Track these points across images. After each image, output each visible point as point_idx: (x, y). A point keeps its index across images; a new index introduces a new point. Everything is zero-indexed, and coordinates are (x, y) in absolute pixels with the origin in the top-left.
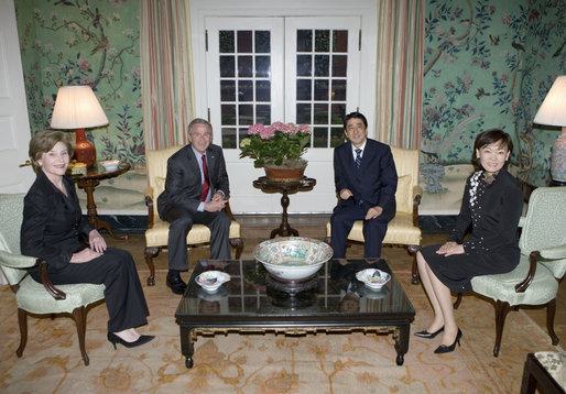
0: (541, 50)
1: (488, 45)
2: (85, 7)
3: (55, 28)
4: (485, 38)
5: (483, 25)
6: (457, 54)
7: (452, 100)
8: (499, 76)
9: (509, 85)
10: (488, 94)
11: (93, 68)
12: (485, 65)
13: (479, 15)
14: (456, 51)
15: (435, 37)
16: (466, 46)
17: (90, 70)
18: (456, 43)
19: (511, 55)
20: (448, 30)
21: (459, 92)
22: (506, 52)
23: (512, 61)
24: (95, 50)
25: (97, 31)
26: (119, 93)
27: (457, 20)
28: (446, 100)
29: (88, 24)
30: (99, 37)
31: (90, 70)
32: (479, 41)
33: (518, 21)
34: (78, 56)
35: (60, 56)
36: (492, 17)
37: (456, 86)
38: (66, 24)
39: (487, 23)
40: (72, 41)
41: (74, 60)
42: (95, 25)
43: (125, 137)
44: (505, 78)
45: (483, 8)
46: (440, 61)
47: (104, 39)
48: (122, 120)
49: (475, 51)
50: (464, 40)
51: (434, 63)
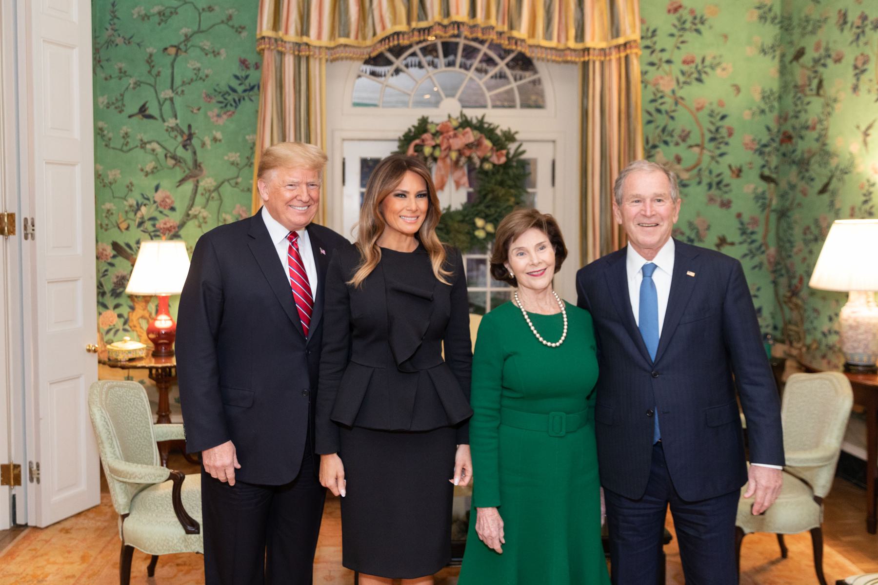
0: (801, 185)
1: (727, 177)
2: (172, 122)
3: (125, 148)
4: (722, 167)
5: (718, 152)
8: (746, 218)
9: (760, 230)
10: (732, 244)
11: (176, 205)
12: (726, 204)
13: (713, 139)
16: (697, 180)
17: (173, 209)
19: (760, 190)
20: (672, 158)
22: (752, 186)
23: (760, 198)
24: (182, 181)
25: (187, 155)
27: (683, 146)
29: (175, 145)
30: (190, 163)
31: (173, 209)
32: (715, 172)
33: (765, 146)
34: (157, 188)
35: (130, 187)
36: (731, 140)
38: (143, 144)
39: (724, 148)
40: (149, 167)
41: (150, 193)
42: (184, 146)
44: (755, 221)
45: (717, 130)
47: (197, 165)
49: (710, 186)
50: (695, 171)
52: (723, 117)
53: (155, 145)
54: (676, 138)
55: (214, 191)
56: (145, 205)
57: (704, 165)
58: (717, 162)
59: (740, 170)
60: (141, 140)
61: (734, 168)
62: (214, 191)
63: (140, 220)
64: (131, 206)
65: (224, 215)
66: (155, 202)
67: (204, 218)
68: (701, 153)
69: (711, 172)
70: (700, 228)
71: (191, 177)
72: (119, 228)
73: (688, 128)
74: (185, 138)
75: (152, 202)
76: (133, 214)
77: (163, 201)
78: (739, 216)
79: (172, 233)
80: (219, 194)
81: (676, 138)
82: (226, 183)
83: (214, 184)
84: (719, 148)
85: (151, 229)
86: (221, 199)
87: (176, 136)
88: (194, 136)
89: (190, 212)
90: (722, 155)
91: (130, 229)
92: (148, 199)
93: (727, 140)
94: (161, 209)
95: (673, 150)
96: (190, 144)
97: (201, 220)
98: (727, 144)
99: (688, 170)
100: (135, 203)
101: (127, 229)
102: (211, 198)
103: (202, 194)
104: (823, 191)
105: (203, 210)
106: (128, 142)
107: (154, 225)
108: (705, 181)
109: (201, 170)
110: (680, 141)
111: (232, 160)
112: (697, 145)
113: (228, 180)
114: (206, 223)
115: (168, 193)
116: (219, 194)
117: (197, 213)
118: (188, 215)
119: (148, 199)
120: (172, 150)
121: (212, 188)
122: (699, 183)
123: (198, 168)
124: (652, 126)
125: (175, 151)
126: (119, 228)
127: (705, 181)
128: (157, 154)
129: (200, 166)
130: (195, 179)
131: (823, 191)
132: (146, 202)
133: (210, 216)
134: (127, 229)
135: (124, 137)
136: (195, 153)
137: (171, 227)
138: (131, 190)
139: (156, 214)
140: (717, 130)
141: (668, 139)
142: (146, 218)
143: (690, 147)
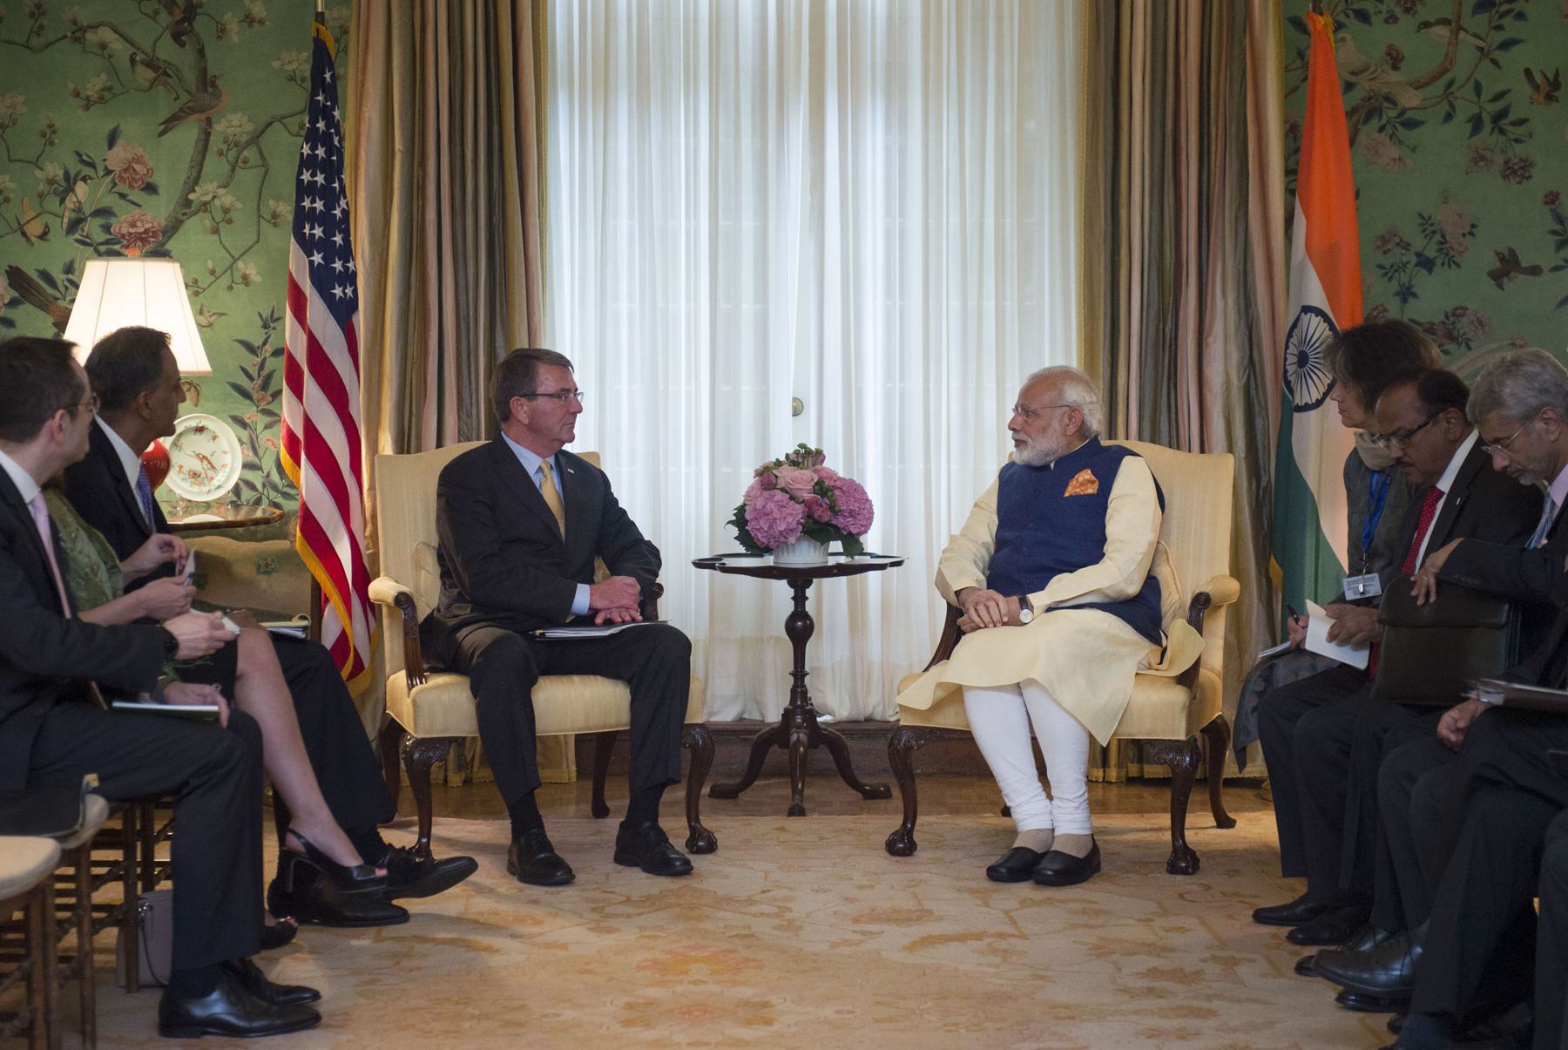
1: (1521, 100)
3: (35, 41)
5: (1499, 37)
6: (1411, 136)
7: (1406, 294)
10: (1535, 271)
11: (159, 179)
12: (1518, 171)
14: (1411, 124)
16: (1445, 107)
17: (151, 189)
18: (1410, 99)
21: (1426, 264)
24: (170, 123)
26: (249, 267)
27: (1406, 22)
30: (191, 78)
31: (151, 189)
34: (112, 140)
35: (49, 136)
37: (1418, 243)
38: (78, 33)
39: (1512, 28)
40: (93, 87)
41: (96, 151)
42: (176, 37)
43: (264, 420)
47: (207, 82)
48: (251, 362)
49: (1476, 124)
50: (1438, 88)
53: (106, 34)
55: (248, 144)
56: (84, 179)
57: (1460, 72)
58: (1495, 63)
59: (1555, 84)
60: (74, 22)
61: (1538, 78)
62: (248, 144)
63: (74, 215)
64: (51, 182)
65: (272, 203)
66: (108, 172)
67: (226, 211)
68: (1454, 41)
69: (1478, 89)
70: (1448, 230)
71: (193, 111)
72: (24, 234)
74: (178, 16)
75: (101, 173)
76: (57, 200)
77: (126, 170)
78: (1552, 198)
79: (149, 247)
80: (261, 153)
82: (277, 125)
83: (249, 127)
84: (1499, 28)
85: (99, 236)
86: (264, 164)
87: (156, 13)
88: (199, 11)
89: (192, 196)
90: (1506, 45)
91: (50, 236)
92: (92, 165)
94: (122, 188)
96: (191, 31)
97: (219, 216)
99: (1418, 86)
100: (61, 173)
101: (44, 236)
102: (240, 164)
103: (221, 153)
105: (221, 191)
106: (41, 27)
107: (107, 228)
108: (1464, 111)
109: (217, 94)
110: (1398, 11)
111: (289, 68)
112: (1444, 22)
113: (281, 119)
114: (230, 222)
115: (140, 151)
116: (261, 153)
117: (208, 198)
118: (187, 203)
119: (92, 165)
120: (147, 45)
121: (244, 138)
122: (1449, 117)
123: (210, 90)
125: (154, 50)
126: (24, 234)
127: (1464, 111)
128: (110, 56)
129: (213, 85)
130: (203, 116)
132: (87, 171)
133: (239, 205)
134: (44, 236)
135: (32, 15)
136: (201, 52)
137: (146, 231)
138: (52, 144)
139: (110, 201)
142: (87, 211)
143: (1426, 25)
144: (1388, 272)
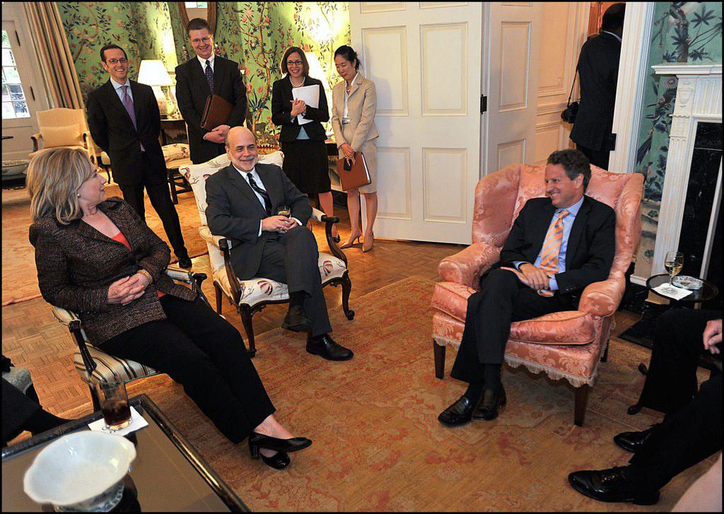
5: (106, 28)
13: (101, 22)
15: (75, 37)
18: (91, 40)
19: (130, 47)
28: (95, 78)
33: (128, 25)
37: (100, 68)
39: (108, 26)
45: (103, 17)
46: (83, 52)
51: (79, 53)
52: (104, 11)
54: (82, 21)
59: (119, 37)
69: (104, 38)
73: (87, 16)
81: (82, 21)
90: (108, 30)
93: (109, 22)
95: (82, 27)
98: (109, 24)
104: (151, 48)
124: (68, 14)
131: (151, 48)
140: (103, 17)
141: (78, 21)
144: (95, 74)
